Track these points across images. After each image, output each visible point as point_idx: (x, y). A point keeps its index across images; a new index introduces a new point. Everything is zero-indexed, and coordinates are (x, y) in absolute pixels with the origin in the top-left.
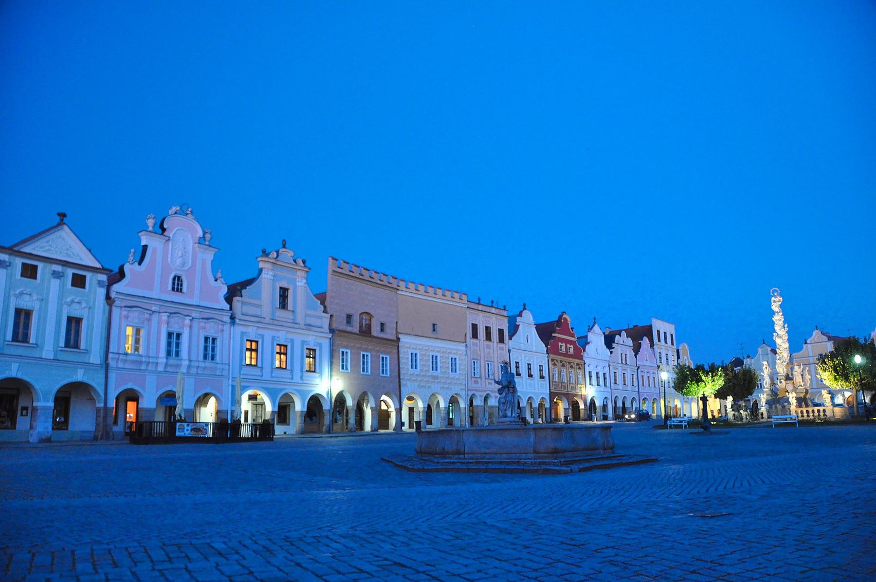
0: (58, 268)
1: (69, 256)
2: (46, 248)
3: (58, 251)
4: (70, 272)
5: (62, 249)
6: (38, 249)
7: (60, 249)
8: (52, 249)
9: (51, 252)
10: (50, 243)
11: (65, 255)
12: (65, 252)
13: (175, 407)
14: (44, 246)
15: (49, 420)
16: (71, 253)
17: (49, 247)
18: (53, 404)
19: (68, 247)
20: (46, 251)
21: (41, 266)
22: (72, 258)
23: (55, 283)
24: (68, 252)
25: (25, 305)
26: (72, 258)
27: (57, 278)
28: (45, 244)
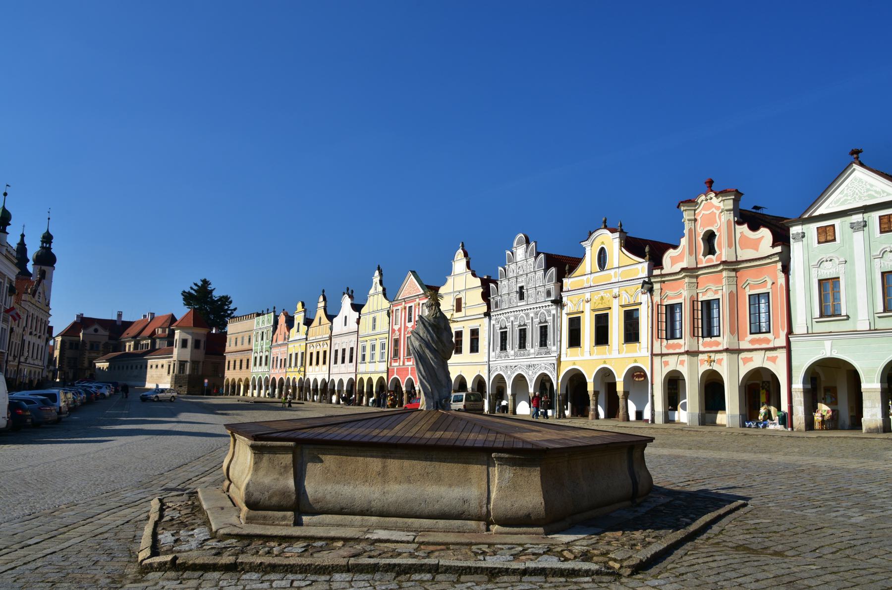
0: (857, 218)
1: (873, 197)
2: (842, 200)
3: (857, 197)
4: (874, 217)
5: (861, 193)
6: (833, 205)
7: (859, 194)
8: (849, 198)
9: (849, 202)
10: (845, 192)
11: (867, 198)
12: (865, 194)
13: (615, 384)
14: (840, 199)
15: (877, 405)
16: (873, 193)
17: (845, 198)
18: (880, 384)
19: (868, 187)
20: (842, 204)
21: (837, 222)
22: (877, 198)
23: (859, 236)
24: (869, 193)
25: (828, 274)
26: (877, 198)
27: (858, 230)
28: (841, 196)
